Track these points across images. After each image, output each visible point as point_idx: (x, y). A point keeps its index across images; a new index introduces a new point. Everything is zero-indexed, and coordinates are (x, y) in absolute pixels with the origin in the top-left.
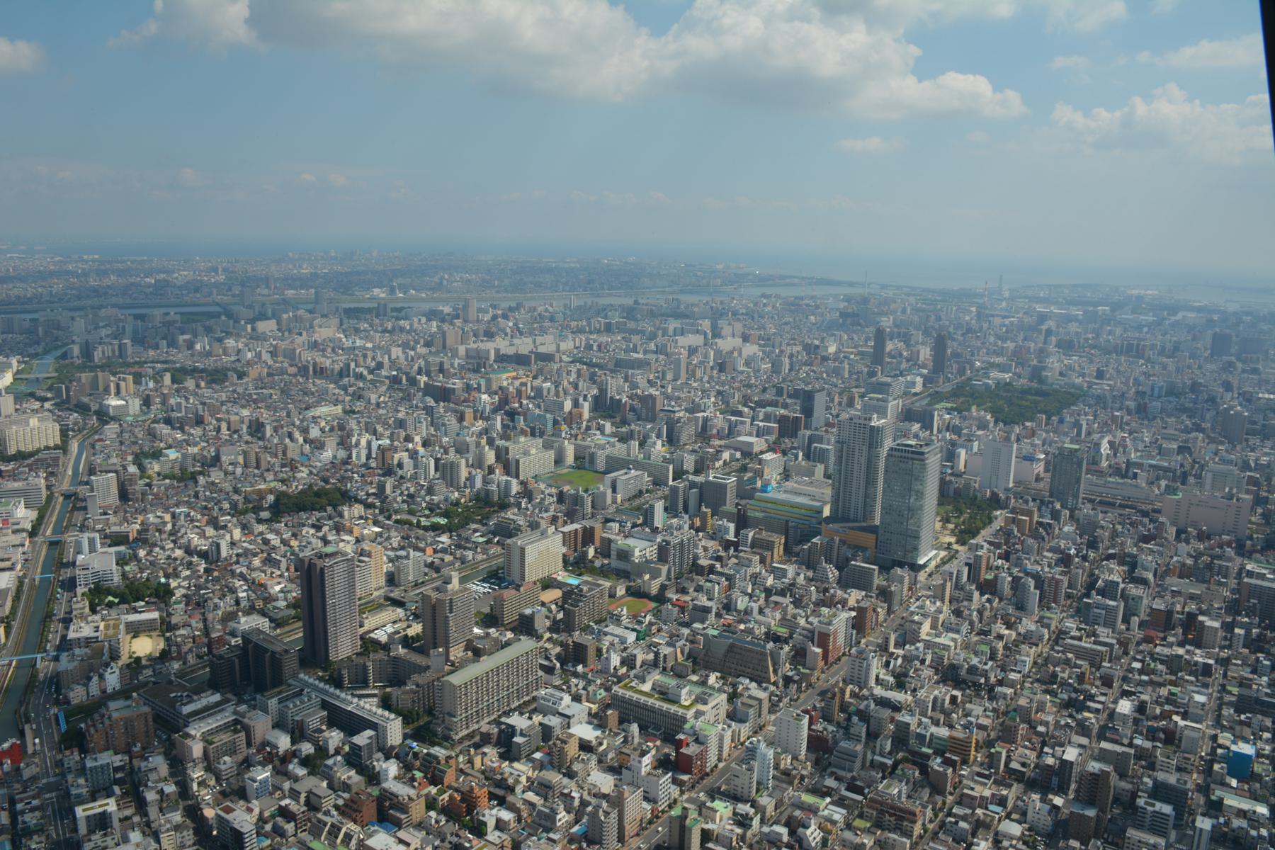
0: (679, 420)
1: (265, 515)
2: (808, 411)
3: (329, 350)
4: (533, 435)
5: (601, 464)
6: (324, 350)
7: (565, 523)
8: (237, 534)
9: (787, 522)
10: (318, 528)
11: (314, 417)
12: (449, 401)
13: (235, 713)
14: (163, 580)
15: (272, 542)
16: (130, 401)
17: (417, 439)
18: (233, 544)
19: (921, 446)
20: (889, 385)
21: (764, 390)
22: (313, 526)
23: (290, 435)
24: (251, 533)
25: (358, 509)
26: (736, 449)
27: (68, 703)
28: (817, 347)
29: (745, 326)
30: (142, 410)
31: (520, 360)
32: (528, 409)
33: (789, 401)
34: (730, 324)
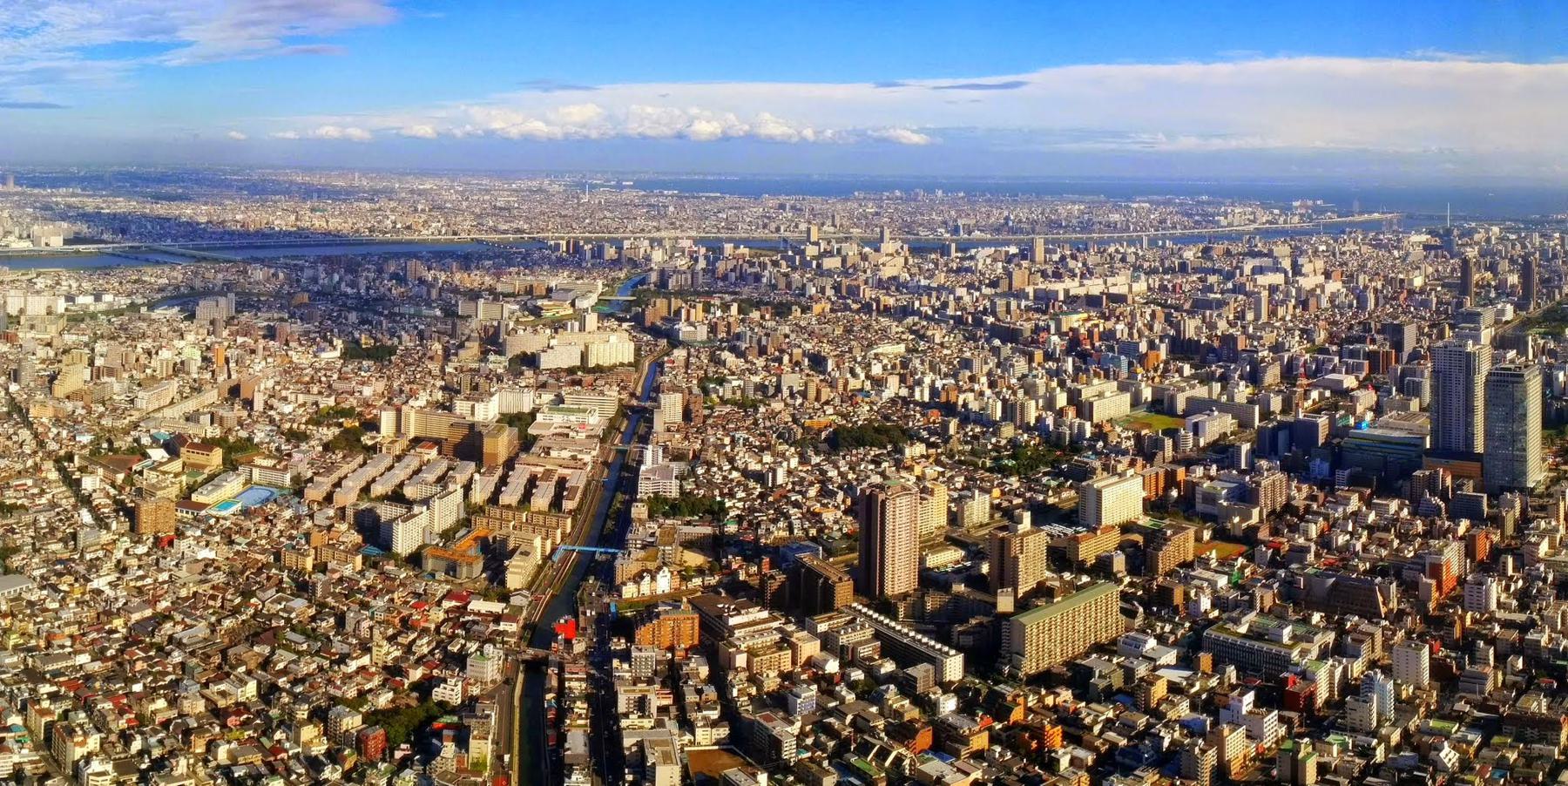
0: (1263, 360)
1: (824, 447)
3: (893, 288)
4: (1107, 377)
5: (1181, 405)
6: (888, 289)
8: (794, 462)
10: (876, 462)
11: (876, 355)
15: (830, 474)
18: (790, 472)
21: (1351, 327)
22: (873, 462)
23: (852, 372)
24: (809, 463)
25: (920, 449)
26: (1325, 388)
31: (1092, 301)
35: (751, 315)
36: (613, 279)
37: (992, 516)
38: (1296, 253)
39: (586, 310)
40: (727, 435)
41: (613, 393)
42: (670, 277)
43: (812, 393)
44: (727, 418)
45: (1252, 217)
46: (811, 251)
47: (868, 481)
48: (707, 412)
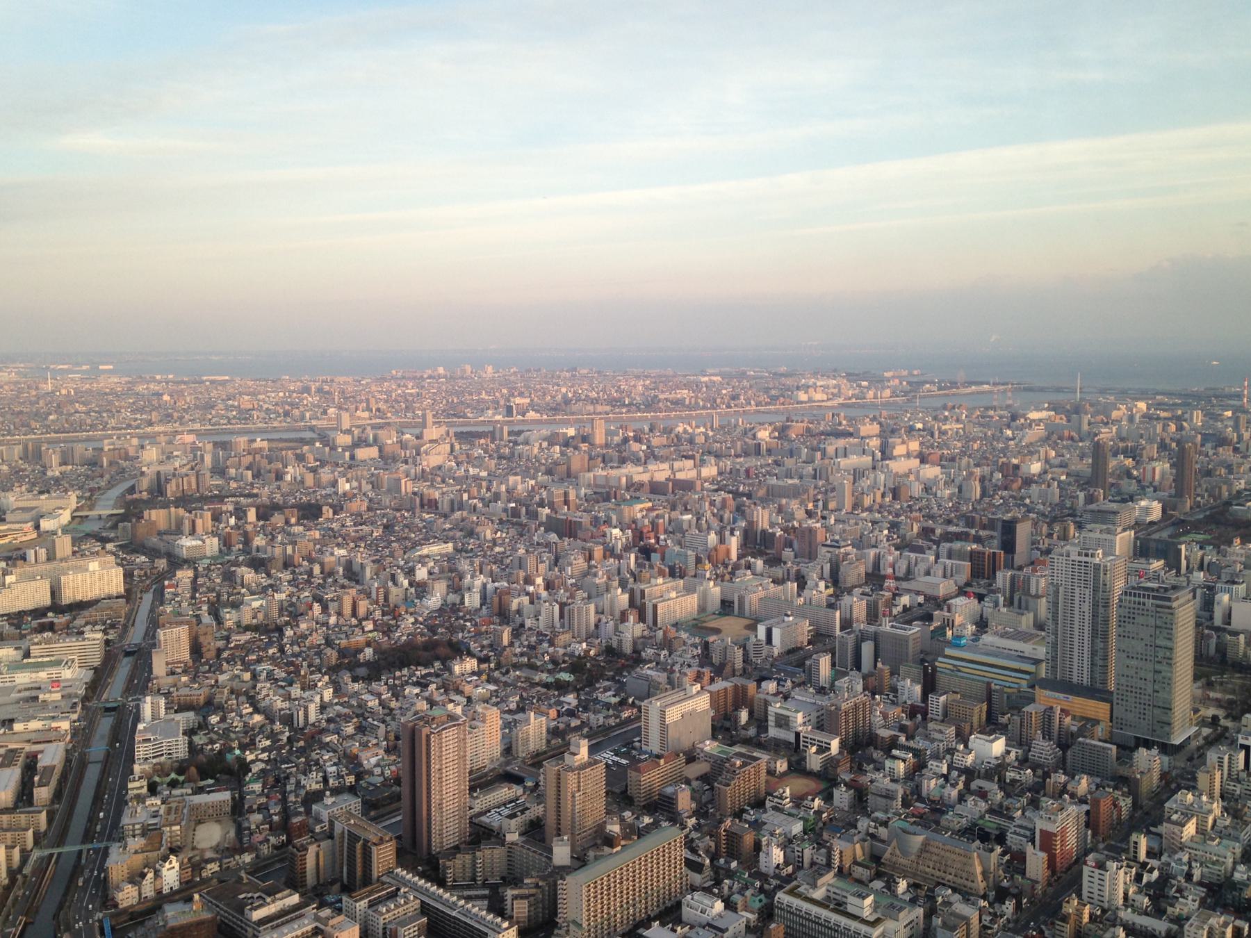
2: (1009, 546)
6: (433, 481)
7: (712, 680)
8: (328, 694)
9: (989, 684)
10: (423, 685)
12: (575, 537)
13: (317, 919)
14: (237, 752)
15: (370, 704)
16: (208, 541)
17: (539, 581)
18: (323, 707)
19: (1166, 590)
20: (1115, 513)
22: (417, 684)
23: (393, 578)
25: (471, 664)
27: (116, 906)
28: (1017, 467)
29: (921, 444)
30: (220, 551)
31: (656, 488)
32: (667, 546)
33: (982, 533)
34: (903, 443)
35: (273, 520)
36: (92, 490)
37: (548, 742)
38: (887, 433)
39: (54, 533)
40: (246, 670)
41: (95, 637)
42: (168, 481)
43: (347, 610)
44: (246, 648)
45: (836, 391)
46: (343, 440)
47: (413, 709)
48: (221, 644)
